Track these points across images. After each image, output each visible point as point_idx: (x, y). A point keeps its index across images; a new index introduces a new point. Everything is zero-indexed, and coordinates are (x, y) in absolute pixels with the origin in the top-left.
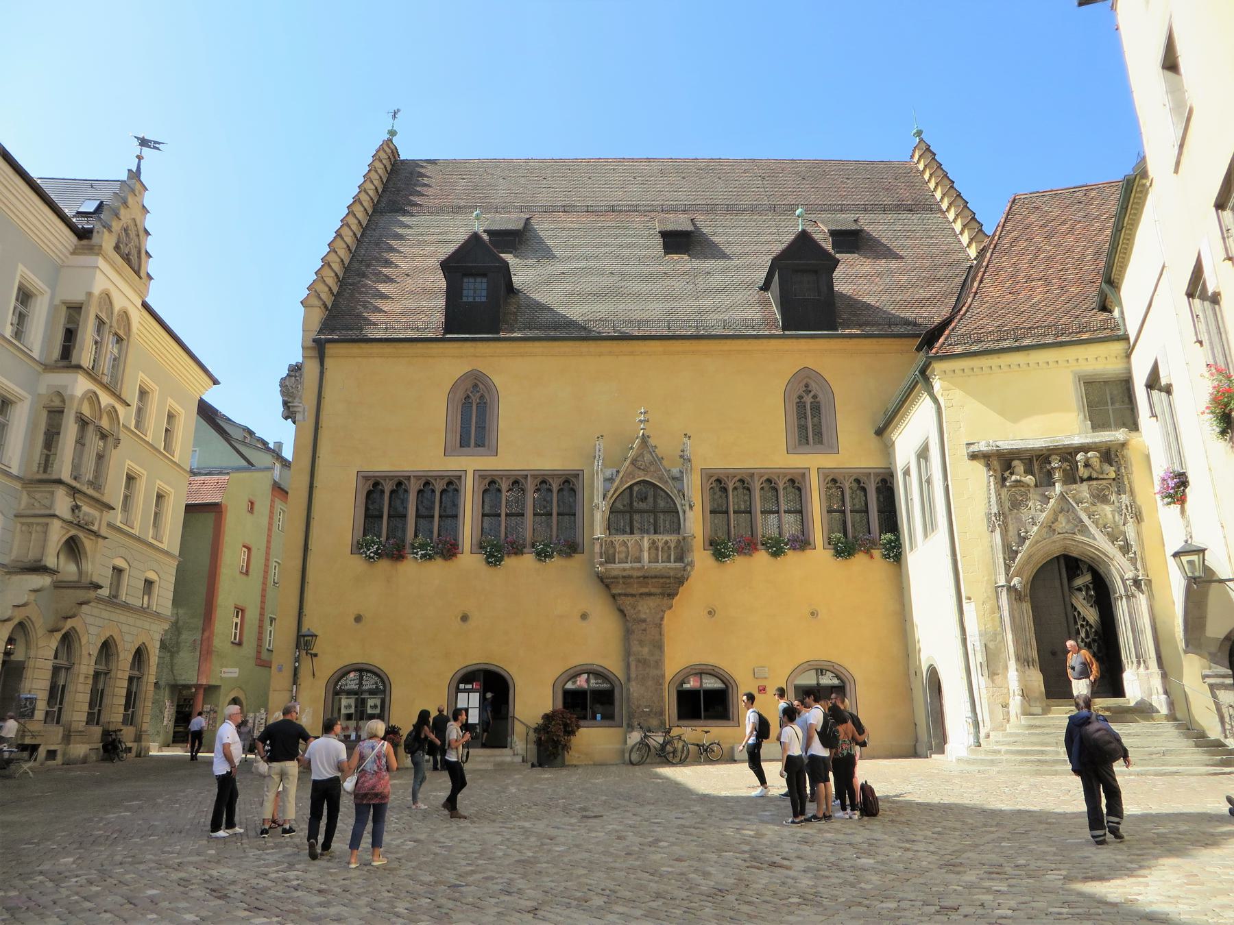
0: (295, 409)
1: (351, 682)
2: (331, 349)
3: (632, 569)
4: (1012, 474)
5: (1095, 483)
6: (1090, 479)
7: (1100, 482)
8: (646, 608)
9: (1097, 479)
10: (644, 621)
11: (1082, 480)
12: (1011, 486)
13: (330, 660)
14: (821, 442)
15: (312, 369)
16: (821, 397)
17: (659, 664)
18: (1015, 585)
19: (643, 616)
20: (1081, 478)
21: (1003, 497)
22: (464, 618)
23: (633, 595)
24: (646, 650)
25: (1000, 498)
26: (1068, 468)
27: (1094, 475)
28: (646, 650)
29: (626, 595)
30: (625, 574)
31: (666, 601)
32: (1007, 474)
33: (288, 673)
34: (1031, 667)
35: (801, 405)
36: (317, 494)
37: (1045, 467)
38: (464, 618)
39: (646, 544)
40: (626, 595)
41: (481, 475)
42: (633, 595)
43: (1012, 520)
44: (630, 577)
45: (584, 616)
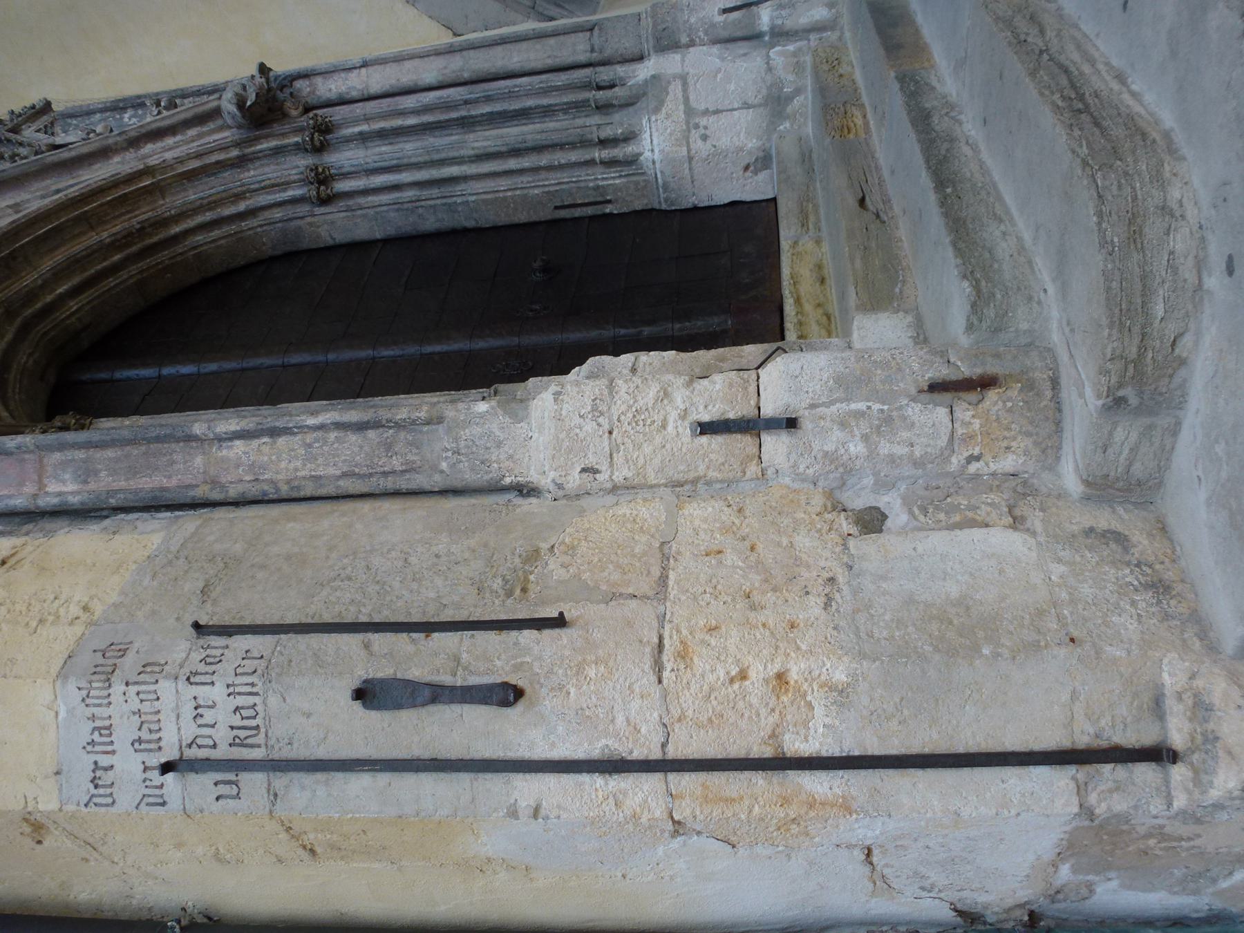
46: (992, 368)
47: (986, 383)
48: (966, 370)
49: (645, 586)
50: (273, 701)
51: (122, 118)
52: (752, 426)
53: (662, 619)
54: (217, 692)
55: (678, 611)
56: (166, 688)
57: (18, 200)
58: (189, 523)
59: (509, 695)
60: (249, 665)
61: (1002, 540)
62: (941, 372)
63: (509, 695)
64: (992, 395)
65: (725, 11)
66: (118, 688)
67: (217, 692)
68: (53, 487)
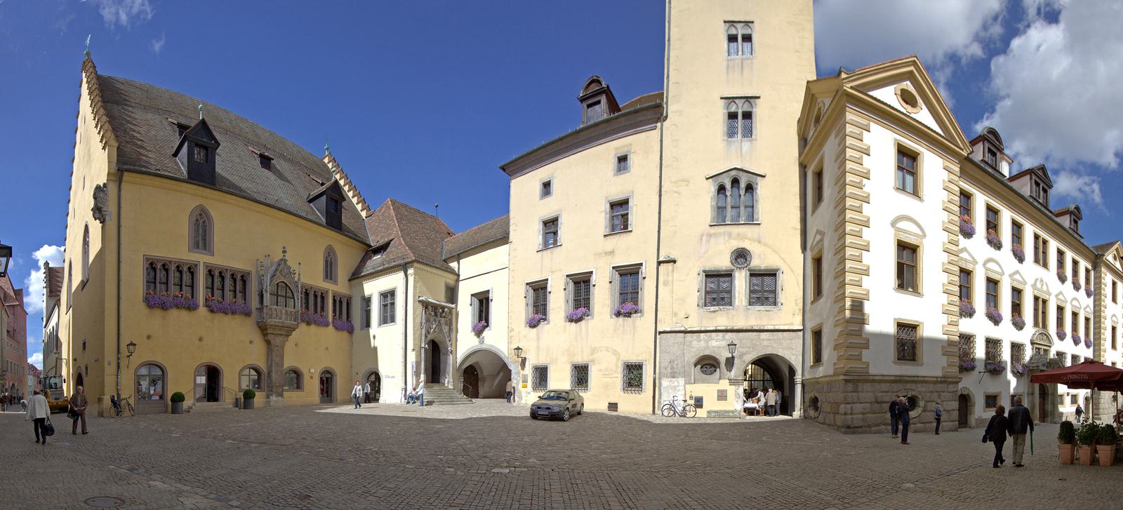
0: (107, 213)
1: (144, 371)
2: (127, 176)
3: (279, 322)
8: (278, 340)
10: (277, 346)
13: (136, 360)
14: (331, 279)
15: (112, 189)
16: (333, 259)
17: (282, 365)
19: (277, 344)
22: (201, 339)
23: (274, 334)
24: (278, 359)
28: (278, 359)
29: (272, 334)
30: (276, 324)
31: (286, 338)
33: (114, 365)
35: (327, 261)
36: (123, 266)
38: (201, 339)
39: (284, 312)
40: (272, 334)
41: (206, 265)
42: (274, 334)
44: (277, 326)
45: (251, 342)
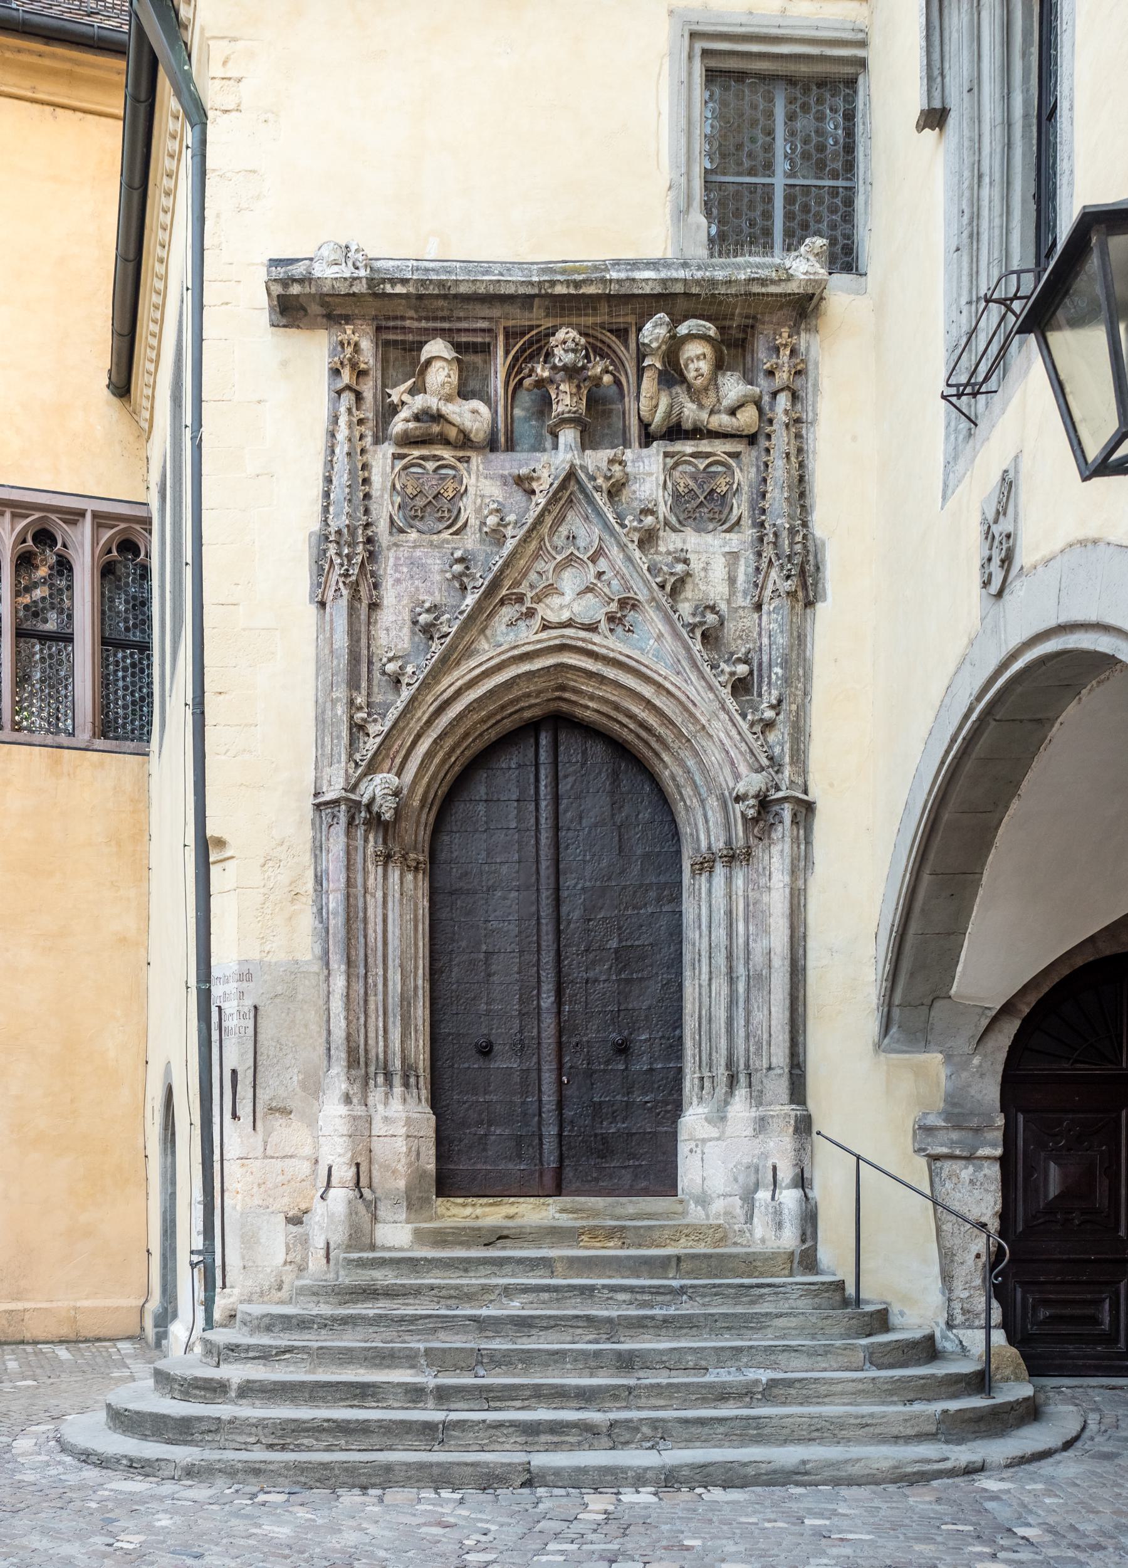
4: (418, 389)
5: (688, 447)
6: (675, 432)
7: (705, 446)
9: (698, 433)
11: (648, 438)
12: (407, 440)
18: (373, 800)
20: (645, 426)
21: (376, 479)
25: (366, 481)
26: (607, 379)
27: (690, 412)
32: (397, 394)
34: (398, 1090)
37: (532, 370)
43: (396, 566)
46: (332, 1262)
47: (328, 1261)
48: (332, 1255)
49: (269, 1152)
50: (233, 1041)
51: (777, 665)
52: (329, 1185)
53: (257, 1158)
54: (235, 1022)
55: (258, 1163)
56: (235, 1003)
57: (666, 635)
58: (316, 967)
59: (235, 1116)
60: (242, 1030)
61: (281, 1257)
62: (332, 1248)
63: (235, 1116)
64: (325, 1261)
65: (775, 1168)
66: (235, 985)
67: (235, 1022)
68: (331, 897)
